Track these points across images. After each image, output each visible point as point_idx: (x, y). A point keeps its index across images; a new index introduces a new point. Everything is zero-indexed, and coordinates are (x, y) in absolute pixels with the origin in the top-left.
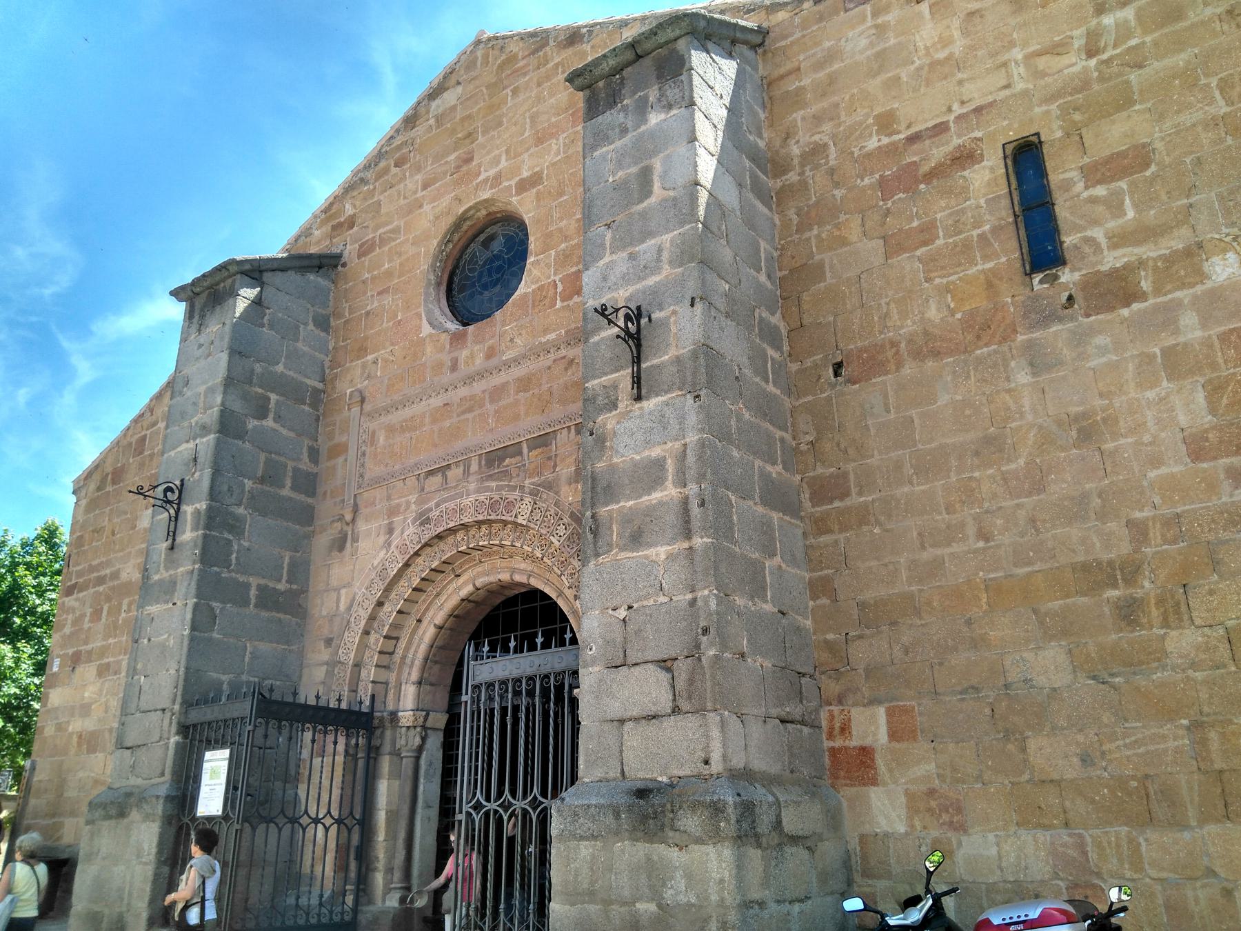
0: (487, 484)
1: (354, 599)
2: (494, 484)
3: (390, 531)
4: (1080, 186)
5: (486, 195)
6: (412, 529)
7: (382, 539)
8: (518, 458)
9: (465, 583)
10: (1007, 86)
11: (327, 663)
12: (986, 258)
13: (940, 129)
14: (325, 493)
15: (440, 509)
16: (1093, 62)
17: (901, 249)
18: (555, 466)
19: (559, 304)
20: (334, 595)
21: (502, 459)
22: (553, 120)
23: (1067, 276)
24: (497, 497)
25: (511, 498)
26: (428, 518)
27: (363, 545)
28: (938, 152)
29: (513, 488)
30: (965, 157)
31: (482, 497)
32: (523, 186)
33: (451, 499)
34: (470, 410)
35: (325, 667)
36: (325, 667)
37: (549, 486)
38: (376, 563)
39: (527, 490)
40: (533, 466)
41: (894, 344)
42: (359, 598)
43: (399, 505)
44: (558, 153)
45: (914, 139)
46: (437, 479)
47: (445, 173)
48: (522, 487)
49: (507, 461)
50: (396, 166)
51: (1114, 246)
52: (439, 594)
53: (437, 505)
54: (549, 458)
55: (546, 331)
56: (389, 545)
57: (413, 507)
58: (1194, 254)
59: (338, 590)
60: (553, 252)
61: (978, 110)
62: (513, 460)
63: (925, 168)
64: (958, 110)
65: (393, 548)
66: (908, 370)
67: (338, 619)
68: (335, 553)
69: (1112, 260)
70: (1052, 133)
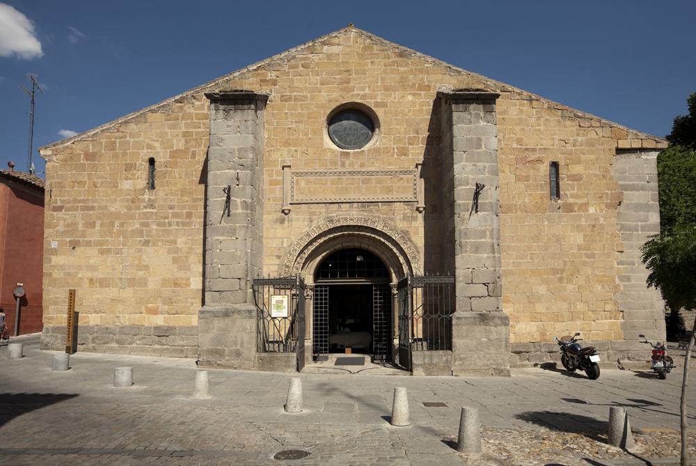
2: (365, 214)
4: (566, 179)
5: (359, 101)
7: (306, 223)
10: (553, 145)
11: (279, 265)
12: (542, 190)
13: (534, 150)
14: (269, 199)
16: (573, 148)
17: (520, 180)
18: (394, 213)
19: (395, 156)
22: (393, 84)
23: (559, 201)
28: (533, 157)
30: (540, 161)
31: (360, 217)
32: (377, 104)
34: (352, 184)
37: (392, 220)
41: (515, 206)
44: (395, 98)
45: (527, 149)
47: (334, 83)
48: (379, 217)
50: (303, 66)
51: (571, 198)
55: (389, 164)
58: (586, 204)
60: (393, 136)
61: (545, 149)
63: (529, 159)
64: (539, 147)
65: (313, 227)
66: (519, 213)
69: (571, 200)
70: (562, 163)
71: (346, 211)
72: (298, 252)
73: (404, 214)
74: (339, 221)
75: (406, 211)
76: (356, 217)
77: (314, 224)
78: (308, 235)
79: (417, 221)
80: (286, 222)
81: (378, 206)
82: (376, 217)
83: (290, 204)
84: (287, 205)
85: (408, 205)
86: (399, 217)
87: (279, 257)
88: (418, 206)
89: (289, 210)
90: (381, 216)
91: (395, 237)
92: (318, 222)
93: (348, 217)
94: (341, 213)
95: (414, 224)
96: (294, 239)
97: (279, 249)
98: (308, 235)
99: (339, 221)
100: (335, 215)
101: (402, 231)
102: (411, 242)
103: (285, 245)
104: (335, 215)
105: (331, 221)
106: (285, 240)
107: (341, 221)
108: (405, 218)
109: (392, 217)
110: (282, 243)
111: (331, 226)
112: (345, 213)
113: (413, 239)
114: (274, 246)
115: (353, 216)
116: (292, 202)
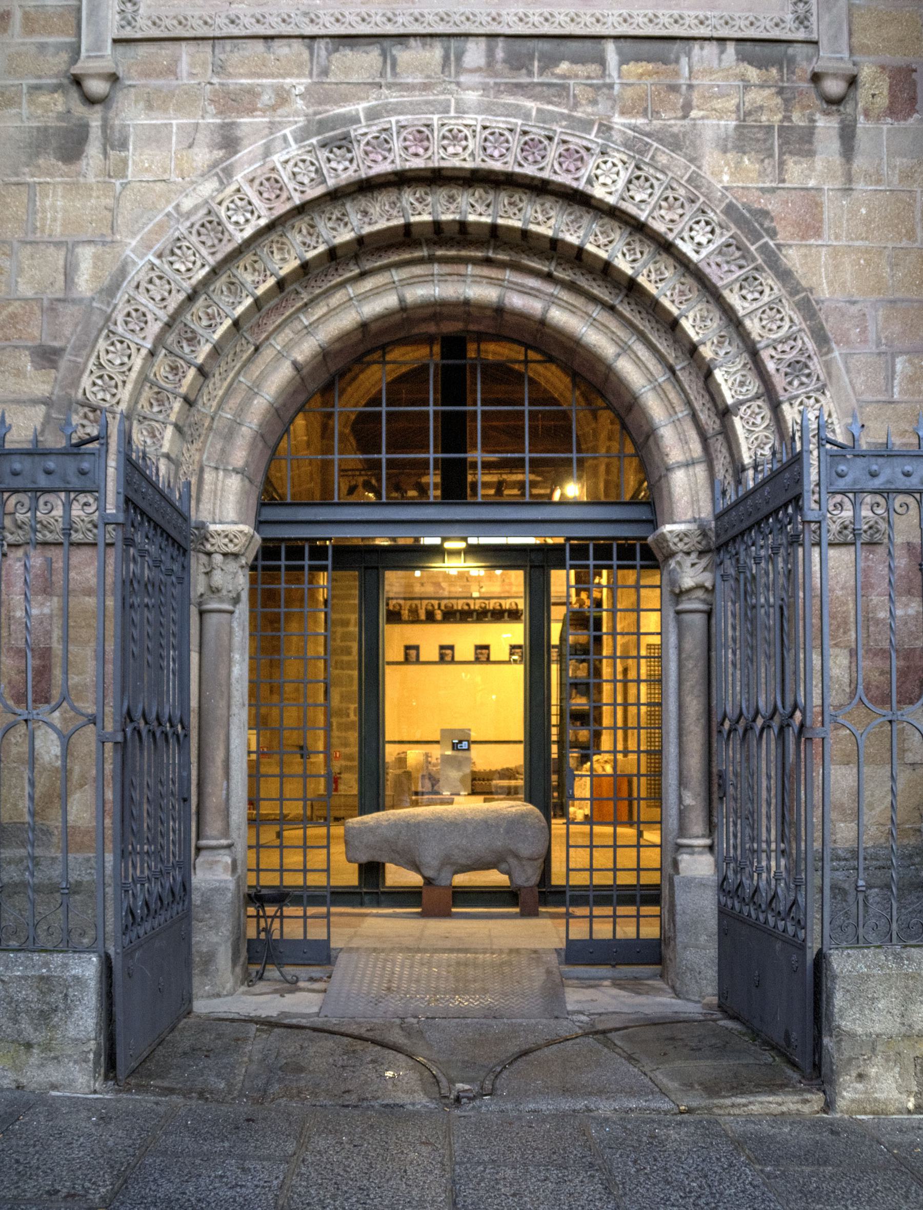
0: (510, 100)
1: (123, 272)
2: (532, 105)
3: (229, 142)
6: (294, 150)
7: (202, 156)
8: (593, 68)
9: (376, 292)
11: (47, 402)
15: (382, 123)
18: (687, 107)
20: (58, 257)
21: (549, 62)
24: (537, 133)
25: (575, 142)
26: (346, 137)
27: (140, 161)
29: (586, 125)
31: (500, 123)
33: (414, 108)
35: (41, 410)
36: (41, 410)
37: (675, 143)
38: (187, 204)
39: (616, 136)
40: (629, 92)
42: (138, 271)
43: (252, 93)
46: (371, 57)
48: (606, 129)
49: (564, 66)
52: (313, 301)
53: (373, 115)
54: (674, 88)
56: (228, 173)
57: (300, 104)
59: (69, 247)
62: (579, 69)
65: (239, 177)
67: (69, 313)
68: (48, 161)
71: (425, 87)
72: (154, 328)
73: (744, 115)
74: (382, 142)
75: (756, 97)
76: (476, 119)
77: (247, 164)
78: (212, 225)
79: (811, 154)
80: (93, 150)
81: (602, 61)
82: (586, 125)
83: (115, 41)
84: (97, 45)
85: (761, 64)
86: (714, 123)
87: (47, 357)
88: (819, 66)
89: (113, 78)
90: (618, 120)
91: (698, 245)
92: (267, 152)
93: (435, 119)
94: (394, 98)
95: (797, 172)
96: (137, 252)
97: (52, 308)
98: (212, 225)
99: (382, 142)
100: (360, 108)
101: (730, 210)
102: (784, 275)
103: (84, 284)
104: (360, 108)
105: (344, 143)
106: (86, 256)
107: (396, 144)
108: (747, 137)
109: (677, 126)
110: (69, 272)
111: (342, 172)
112: (417, 97)
113: (792, 258)
114: (25, 289)
115: (469, 119)
116: (128, 33)
